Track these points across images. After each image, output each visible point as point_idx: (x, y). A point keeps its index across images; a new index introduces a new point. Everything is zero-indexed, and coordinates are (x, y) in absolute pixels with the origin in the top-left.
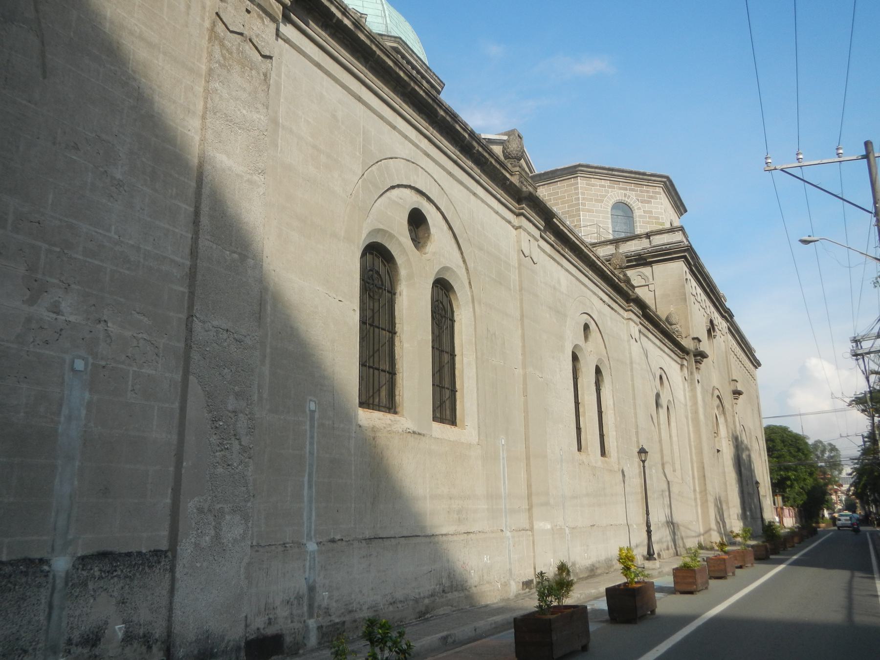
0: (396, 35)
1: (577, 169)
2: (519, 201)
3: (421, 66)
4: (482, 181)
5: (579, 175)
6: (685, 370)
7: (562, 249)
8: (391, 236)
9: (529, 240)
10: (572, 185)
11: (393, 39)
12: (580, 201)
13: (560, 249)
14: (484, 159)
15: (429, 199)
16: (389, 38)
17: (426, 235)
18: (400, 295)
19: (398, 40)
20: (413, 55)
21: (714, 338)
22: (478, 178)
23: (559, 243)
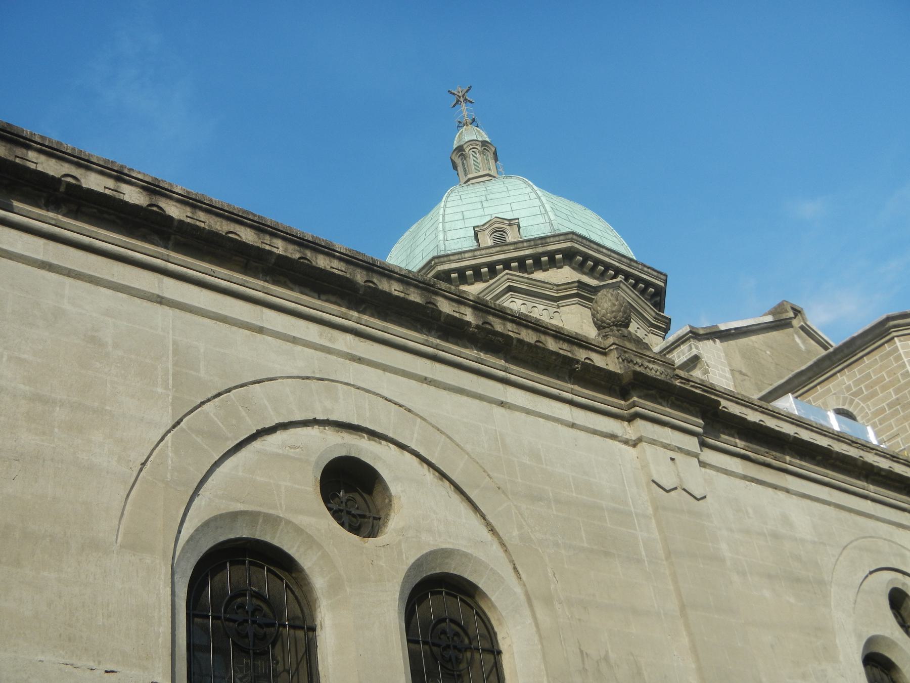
0: (564, 230)
1: (887, 326)
2: (624, 394)
3: (620, 261)
4: (513, 378)
5: (895, 334)
7: (775, 459)
8: (272, 521)
9: (672, 459)
10: (889, 354)
11: (562, 238)
13: (769, 460)
14: (500, 339)
15: (374, 435)
16: (557, 239)
17: (387, 501)
18: (321, 626)
19: (570, 236)
20: (601, 249)
22: (502, 374)
23: (763, 449)
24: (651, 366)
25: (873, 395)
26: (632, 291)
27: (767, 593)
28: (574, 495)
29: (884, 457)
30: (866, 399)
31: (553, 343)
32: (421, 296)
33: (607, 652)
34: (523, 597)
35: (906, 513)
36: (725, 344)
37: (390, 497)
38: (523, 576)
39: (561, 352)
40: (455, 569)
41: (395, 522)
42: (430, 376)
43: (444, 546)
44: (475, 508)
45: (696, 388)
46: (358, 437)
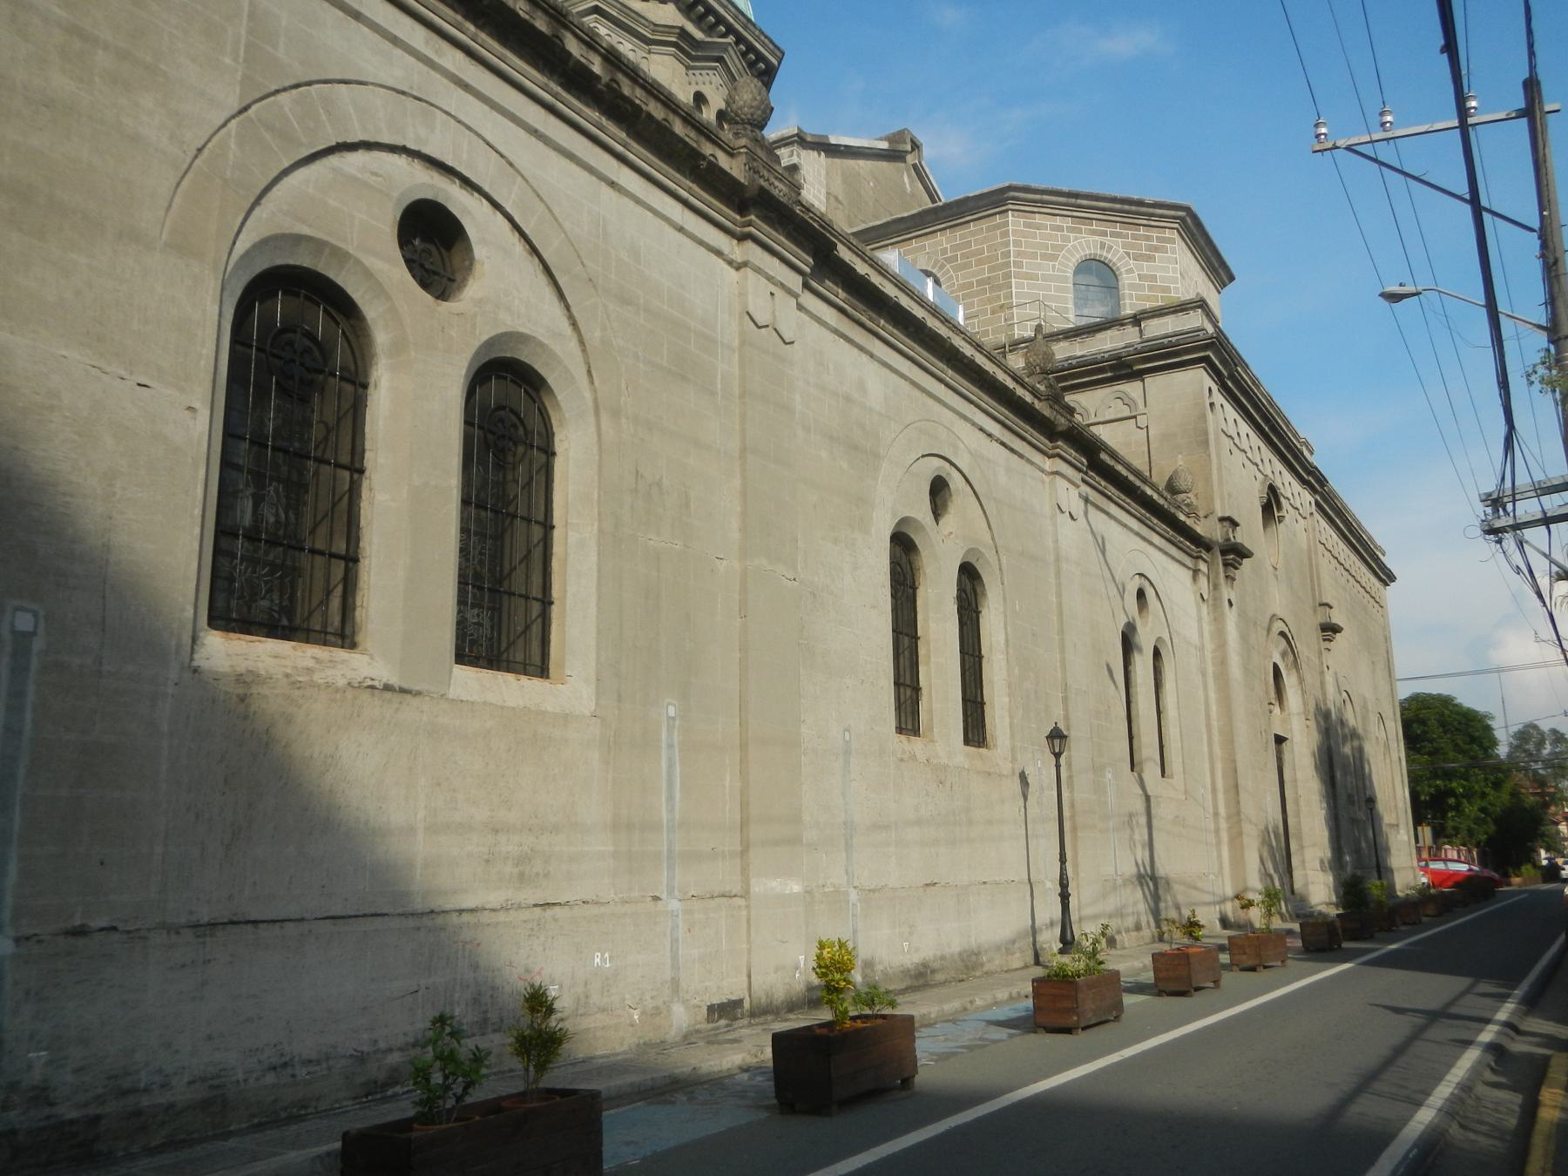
2: (742, 209)
4: (631, 157)
5: (1010, 206)
6: (1203, 581)
7: (871, 319)
8: (341, 256)
9: (772, 294)
10: (998, 227)
12: (1012, 258)
13: (864, 319)
14: (629, 108)
15: (466, 182)
17: (467, 263)
18: (376, 386)
21: (1280, 522)
22: (620, 148)
23: (861, 306)
24: (777, 183)
25: (967, 266)
26: (740, 61)
27: (824, 454)
28: (665, 307)
29: (970, 343)
30: (957, 269)
31: (681, 127)
32: (548, 25)
33: (662, 477)
34: (590, 404)
35: (972, 406)
36: (830, 160)
37: (472, 259)
38: (596, 382)
39: (687, 139)
40: (526, 357)
41: (473, 290)
42: (541, 128)
43: (521, 330)
44: (561, 296)
45: (815, 220)
46: (448, 181)
